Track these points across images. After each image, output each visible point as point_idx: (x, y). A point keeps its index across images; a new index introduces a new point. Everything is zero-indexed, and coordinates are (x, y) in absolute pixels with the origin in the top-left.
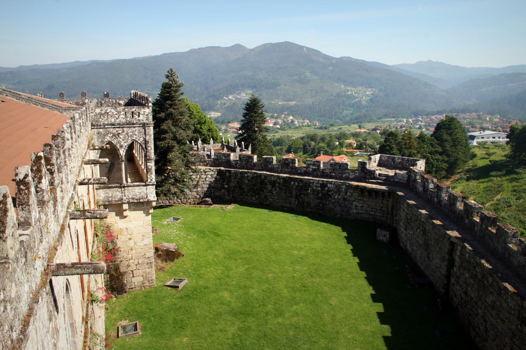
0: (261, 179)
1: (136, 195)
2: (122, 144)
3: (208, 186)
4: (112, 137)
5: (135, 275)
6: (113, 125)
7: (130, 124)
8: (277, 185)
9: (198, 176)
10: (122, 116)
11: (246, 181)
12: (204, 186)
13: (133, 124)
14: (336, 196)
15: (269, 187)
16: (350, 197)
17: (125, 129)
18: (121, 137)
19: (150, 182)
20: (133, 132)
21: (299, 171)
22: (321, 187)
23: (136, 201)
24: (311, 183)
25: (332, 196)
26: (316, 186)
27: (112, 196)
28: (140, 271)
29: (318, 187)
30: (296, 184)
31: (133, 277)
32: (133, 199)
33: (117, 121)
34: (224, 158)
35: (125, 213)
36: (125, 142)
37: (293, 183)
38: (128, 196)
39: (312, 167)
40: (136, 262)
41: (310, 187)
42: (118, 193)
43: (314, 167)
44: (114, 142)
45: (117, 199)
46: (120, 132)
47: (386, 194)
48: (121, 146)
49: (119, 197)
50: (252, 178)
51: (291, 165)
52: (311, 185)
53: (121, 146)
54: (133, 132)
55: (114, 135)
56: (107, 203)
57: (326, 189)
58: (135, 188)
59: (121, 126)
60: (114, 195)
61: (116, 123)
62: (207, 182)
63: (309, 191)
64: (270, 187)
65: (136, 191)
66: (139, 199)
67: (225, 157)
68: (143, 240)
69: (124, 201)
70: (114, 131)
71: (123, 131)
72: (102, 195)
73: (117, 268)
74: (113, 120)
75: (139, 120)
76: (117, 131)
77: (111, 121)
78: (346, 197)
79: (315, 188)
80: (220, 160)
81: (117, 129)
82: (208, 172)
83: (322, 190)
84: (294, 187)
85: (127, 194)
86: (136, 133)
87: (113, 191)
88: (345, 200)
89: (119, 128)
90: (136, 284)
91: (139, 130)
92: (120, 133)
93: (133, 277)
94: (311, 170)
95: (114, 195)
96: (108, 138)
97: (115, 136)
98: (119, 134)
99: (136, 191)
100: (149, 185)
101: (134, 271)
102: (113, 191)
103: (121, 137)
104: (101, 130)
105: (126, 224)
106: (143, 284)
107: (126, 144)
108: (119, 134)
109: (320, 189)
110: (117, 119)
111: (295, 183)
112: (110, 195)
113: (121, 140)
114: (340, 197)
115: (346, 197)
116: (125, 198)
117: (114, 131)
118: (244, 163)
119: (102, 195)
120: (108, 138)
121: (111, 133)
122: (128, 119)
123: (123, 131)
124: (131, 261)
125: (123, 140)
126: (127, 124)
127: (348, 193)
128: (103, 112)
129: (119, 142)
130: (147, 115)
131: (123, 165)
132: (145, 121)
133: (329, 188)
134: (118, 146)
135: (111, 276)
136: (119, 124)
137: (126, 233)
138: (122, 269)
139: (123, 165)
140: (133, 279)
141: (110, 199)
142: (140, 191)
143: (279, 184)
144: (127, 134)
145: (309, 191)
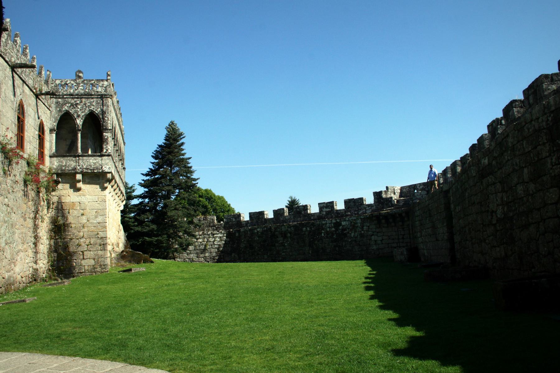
0: (271, 232)
1: (91, 166)
2: (79, 113)
3: (216, 250)
4: (70, 106)
5: (85, 257)
6: (72, 95)
7: (88, 95)
8: (289, 235)
9: (206, 240)
10: (81, 88)
11: (257, 238)
12: (212, 250)
13: (92, 95)
14: (353, 234)
15: (281, 239)
16: (368, 231)
17: (84, 100)
18: (79, 107)
19: (106, 152)
20: (90, 103)
21: (312, 218)
22: (334, 227)
23: (90, 171)
24: (323, 224)
25: (348, 235)
26: (329, 228)
27: (65, 165)
28: (92, 253)
29: (332, 227)
30: (308, 229)
31: (84, 259)
32: (87, 169)
33: (76, 92)
34: (234, 220)
35: (80, 185)
36: (82, 112)
37: (304, 229)
38: (82, 166)
39: (325, 210)
40: (87, 242)
41: (323, 229)
42: (72, 162)
43: (328, 210)
44: (72, 111)
45: (71, 169)
46: (78, 102)
47: (404, 215)
48: (79, 116)
49: (73, 166)
50: (262, 233)
51: (303, 213)
52: (324, 226)
53: (79, 116)
54: (90, 103)
55: (72, 105)
56: (59, 172)
57: (341, 227)
58: (90, 158)
59: (80, 96)
60: (68, 164)
61: (75, 94)
62: (216, 246)
63: (323, 235)
64: (282, 239)
65: (91, 161)
66: (94, 170)
67: (235, 219)
68: (96, 217)
69: (78, 171)
70: (73, 101)
71: (81, 102)
72: (56, 163)
73: (66, 247)
74: (72, 91)
75: (97, 92)
76: (75, 102)
77: (70, 92)
78: (363, 232)
79: (328, 230)
80: (230, 223)
81: (75, 99)
82: (216, 234)
83: (337, 230)
84: (307, 233)
85: (82, 163)
86: (94, 104)
87: (67, 160)
88: (362, 236)
89: (78, 98)
90: (86, 268)
91: (97, 101)
92: (78, 104)
93: (84, 259)
94: (324, 213)
95: (68, 164)
96: (66, 107)
97: (73, 106)
98: (77, 104)
99: (91, 161)
100: (104, 155)
101: (85, 253)
102: (67, 160)
103: (79, 107)
104: (60, 100)
105: (80, 198)
106: (94, 268)
107: (83, 114)
108: (77, 104)
109: (333, 229)
110: (76, 90)
111: (307, 229)
112: (64, 164)
113: (79, 110)
114: (356, 234)
115: (363, 232)
116: (79, 167)
117: (73, 101)
118: (255, 221)
119: (56, 163)
120: (66, 108)
121: (69, 103)
122: (87, 90)
123: (81, 102)
124: (82, 240)
125: (81, 110)
126: (85, 95)
127: (365, 227)
128: (63, 83)
129: (76, 112)
130: (105, 87)
131: (79, 135)
132: (103, 93)
133: (343, 226)
134: (75, 116)
135: (59, 255)
136: (77, 95)
137: (78, 208)
138: (72, 249)
139: (79, 135)
140: (83, 262)
141: (64, 168)
142: (95, 161)
143: (290, 233)
144: (85, 104)
145: (323, 235)
